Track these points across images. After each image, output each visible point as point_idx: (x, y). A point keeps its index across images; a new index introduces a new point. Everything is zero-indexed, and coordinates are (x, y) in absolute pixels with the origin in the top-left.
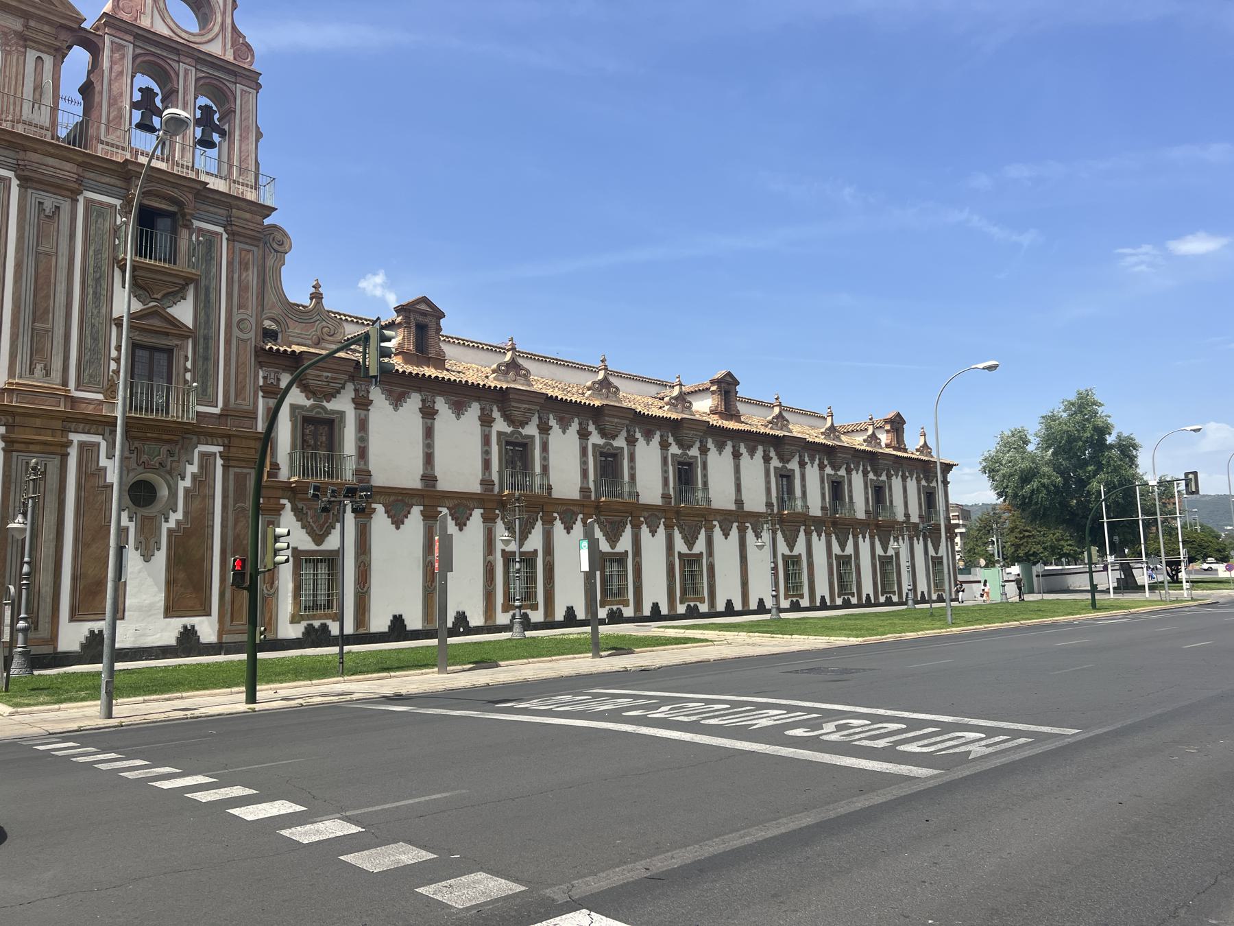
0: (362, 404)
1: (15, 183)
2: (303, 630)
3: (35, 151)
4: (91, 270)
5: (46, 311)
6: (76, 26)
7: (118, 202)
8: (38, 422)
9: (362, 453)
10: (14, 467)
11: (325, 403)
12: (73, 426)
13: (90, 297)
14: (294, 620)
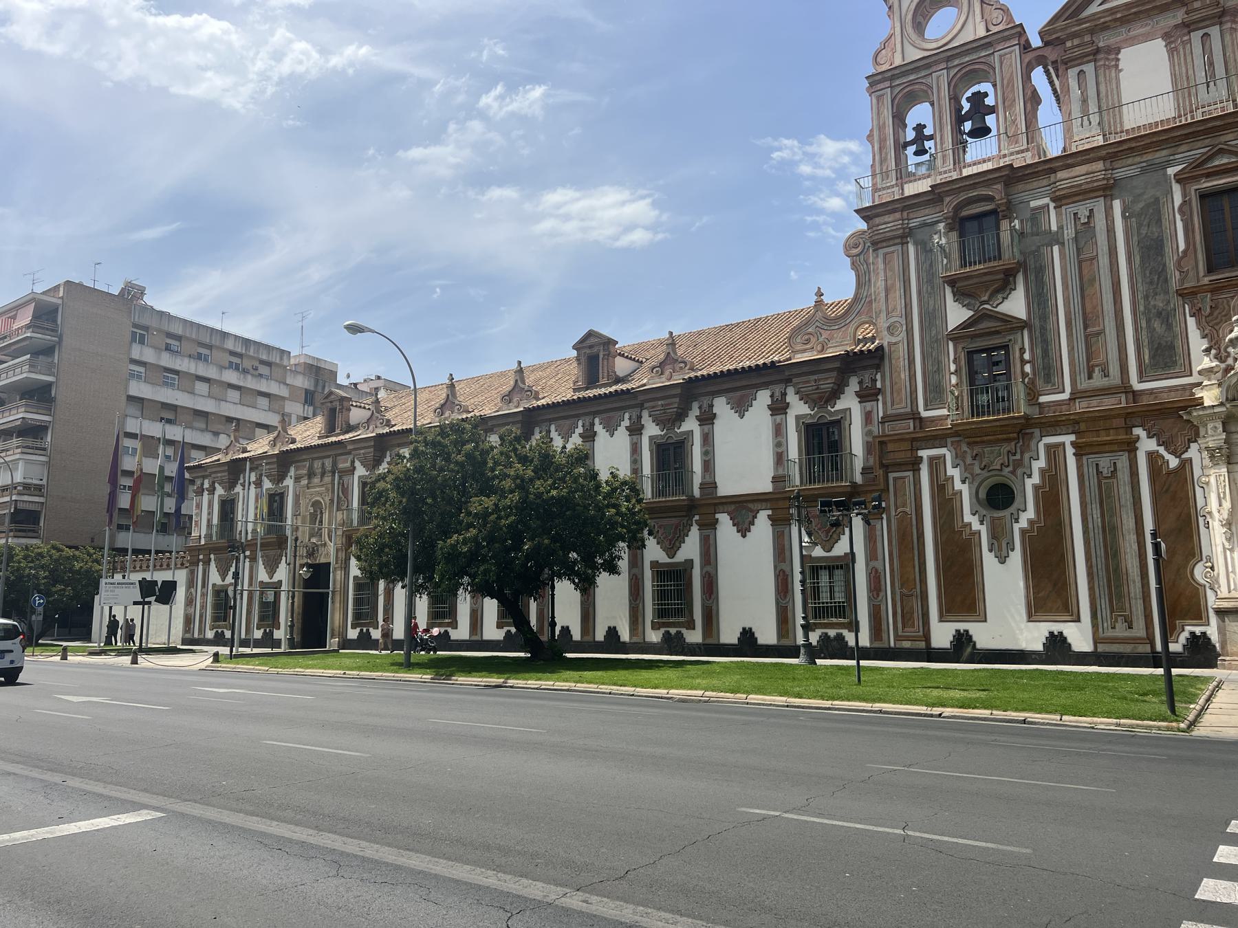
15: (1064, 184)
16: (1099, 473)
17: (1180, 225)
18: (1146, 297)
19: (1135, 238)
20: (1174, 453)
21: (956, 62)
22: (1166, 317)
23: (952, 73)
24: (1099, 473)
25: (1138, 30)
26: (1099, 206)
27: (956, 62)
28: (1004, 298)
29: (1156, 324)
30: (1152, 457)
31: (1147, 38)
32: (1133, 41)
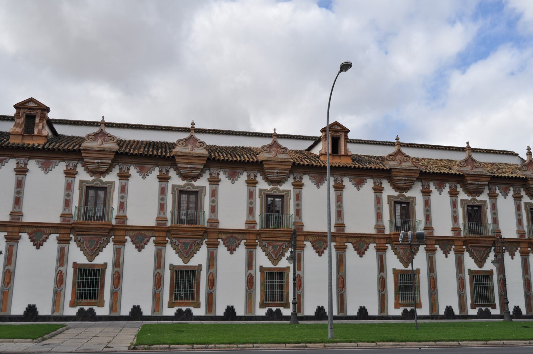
0: (426, 193)
2: (402, 312)
9: (428, 218)
11: (404, 194)
14: (397, 306)
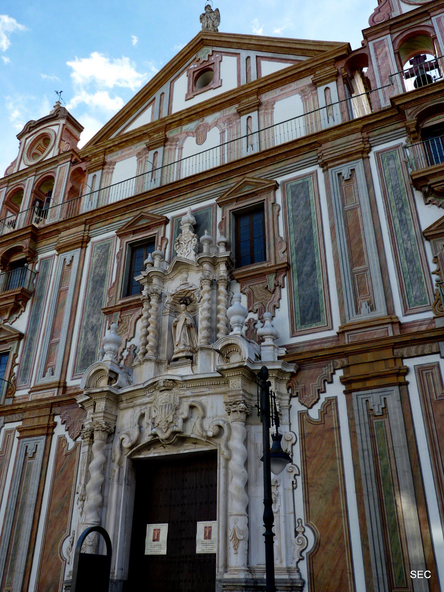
1: (320, 171)
3: (327, 141)
4: (393, 204)
5: (361, 254)
6: (344, 52)
7: (403, 141)
8: (370, 357)
10: (355, 408)
12: (405, 351)
13: (398, 225)
15: (65, 240)
16: (26, 454)
17: (116, 265)
18: (89, 316)
19: (92, 275)
20: (71, 437)
21: (41, 172)
22: (94, 330)
23: (37, 178)
24: (26, 454)
25: (126, 151)
26: (76, 253)
27: (41, 172)
28: (17, 318)
29: (90, 336)
30: (62, 440)
31: (129, 156)
32: (122, 158)
